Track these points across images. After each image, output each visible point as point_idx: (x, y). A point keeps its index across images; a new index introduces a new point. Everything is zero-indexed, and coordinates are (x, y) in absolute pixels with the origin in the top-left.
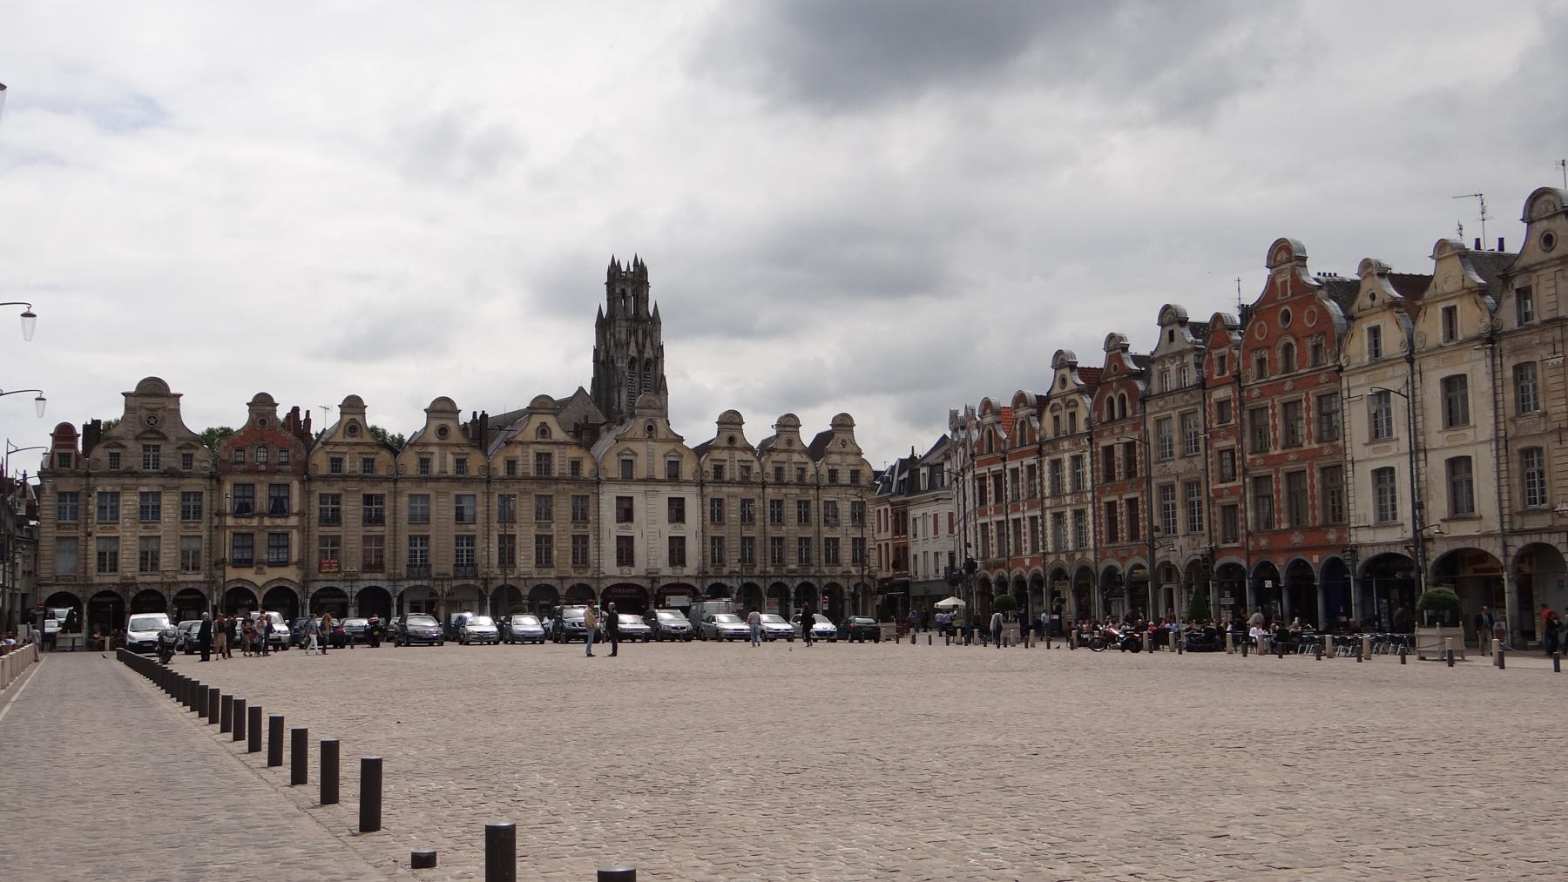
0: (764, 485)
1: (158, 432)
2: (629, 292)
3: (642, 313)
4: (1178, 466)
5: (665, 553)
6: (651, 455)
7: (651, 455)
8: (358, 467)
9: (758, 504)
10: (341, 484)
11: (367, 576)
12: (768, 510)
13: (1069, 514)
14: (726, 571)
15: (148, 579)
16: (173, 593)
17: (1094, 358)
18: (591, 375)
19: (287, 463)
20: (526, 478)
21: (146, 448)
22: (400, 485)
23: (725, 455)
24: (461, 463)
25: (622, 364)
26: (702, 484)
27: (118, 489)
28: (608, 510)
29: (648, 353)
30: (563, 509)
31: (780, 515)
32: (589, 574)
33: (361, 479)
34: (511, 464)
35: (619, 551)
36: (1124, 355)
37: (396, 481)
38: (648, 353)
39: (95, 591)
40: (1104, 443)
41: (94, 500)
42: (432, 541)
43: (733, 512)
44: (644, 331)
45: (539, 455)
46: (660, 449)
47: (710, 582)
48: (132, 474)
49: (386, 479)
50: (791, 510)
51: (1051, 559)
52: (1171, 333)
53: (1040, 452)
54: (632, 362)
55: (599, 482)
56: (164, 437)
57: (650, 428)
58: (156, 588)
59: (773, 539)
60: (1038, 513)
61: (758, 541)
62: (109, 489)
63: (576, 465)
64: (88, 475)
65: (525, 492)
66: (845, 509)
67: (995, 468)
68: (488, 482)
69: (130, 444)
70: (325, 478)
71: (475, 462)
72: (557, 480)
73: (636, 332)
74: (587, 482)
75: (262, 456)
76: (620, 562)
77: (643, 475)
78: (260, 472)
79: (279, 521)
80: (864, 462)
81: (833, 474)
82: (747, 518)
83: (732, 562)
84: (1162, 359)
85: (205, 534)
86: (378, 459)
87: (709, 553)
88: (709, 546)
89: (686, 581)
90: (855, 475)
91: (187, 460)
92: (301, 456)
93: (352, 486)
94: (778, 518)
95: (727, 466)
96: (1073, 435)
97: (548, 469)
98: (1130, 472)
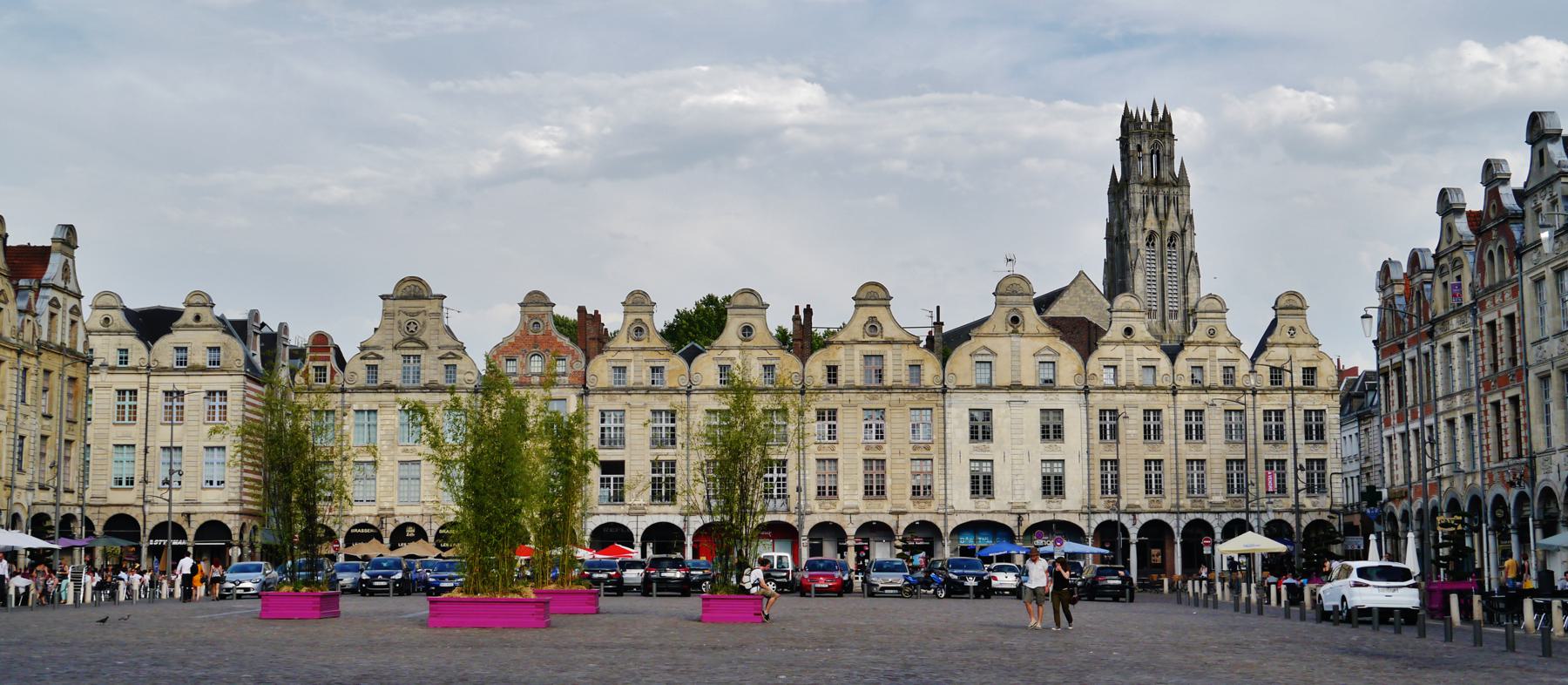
0: (1174, 391)
1: (418, 341)
2: (1146, 149)
3: (1165, 175)
4: (1553, 347)
5: (1037, 483)
6: (1016, 354)
7: (1016, 354)
8: (646, 379)
9: (1167, 415)
10: (626, 398)
11: (655, 509)
13: (1460, 422)
14: (1123, 507)
15: (407, 510)
16: (435, 527)
17: (1475, 200)
19: (564, 374)
20: (851, 387)
22: (693, 397)
23: (1120, 351)
24: (769, 368)
25: (1137, 240)
26: (1086, 391)
27: (375, 407)
28: (958, 427)
29: (1173, 225)
31: (1200, 429)
32: (934, 507)
33: (648, 391)
34: (832, 372)
35: (974, 479)
36: (1502, 190)
37: (688, 393)
38: (1173, 225)
40: (1487, 318)
41: (350, 419)
44: (1167, 198)
46: (1028, 346)
47: (1099, 519)
48: (389, 388)
49: (677, 391)
50: (1215, 424)
51: (1445, 485)
52: (1541, 153)
53: (1430, 334)
55: (944, 391)
56: (426, 347)
57: (1015, 320)
59: (1190, 461)
60: (1430, 421)
61: (1166, 466)
62: (366, 407)
63: (915, 367)
64: (343, 391)
65: (850, 405)
67: (1397, 359)
68: (802, 393)
69: (388, 354)
70: (606, 391)
71: (788, 364)
72: (889, 390)
73: (1155, 199)
74: (927, 389)
75: (536, 366)
76: (975, 491)
77: (1007, 382)
78: (530, 385)
80: (1321, 356)
82: (1152, 432)
83: (1133, 491)
84: (1534, 191)
86: (668, 366)
87: (1097, 482)
88: (1097, 472)
89: (1065, 517)
90: (1310, 374)
92: (579, 367)
93: (636, 399)
94: (1195, 432)
95: (1122, 366)
96: (1459, 311)
97: (880, 375)
98: (1513, 360)
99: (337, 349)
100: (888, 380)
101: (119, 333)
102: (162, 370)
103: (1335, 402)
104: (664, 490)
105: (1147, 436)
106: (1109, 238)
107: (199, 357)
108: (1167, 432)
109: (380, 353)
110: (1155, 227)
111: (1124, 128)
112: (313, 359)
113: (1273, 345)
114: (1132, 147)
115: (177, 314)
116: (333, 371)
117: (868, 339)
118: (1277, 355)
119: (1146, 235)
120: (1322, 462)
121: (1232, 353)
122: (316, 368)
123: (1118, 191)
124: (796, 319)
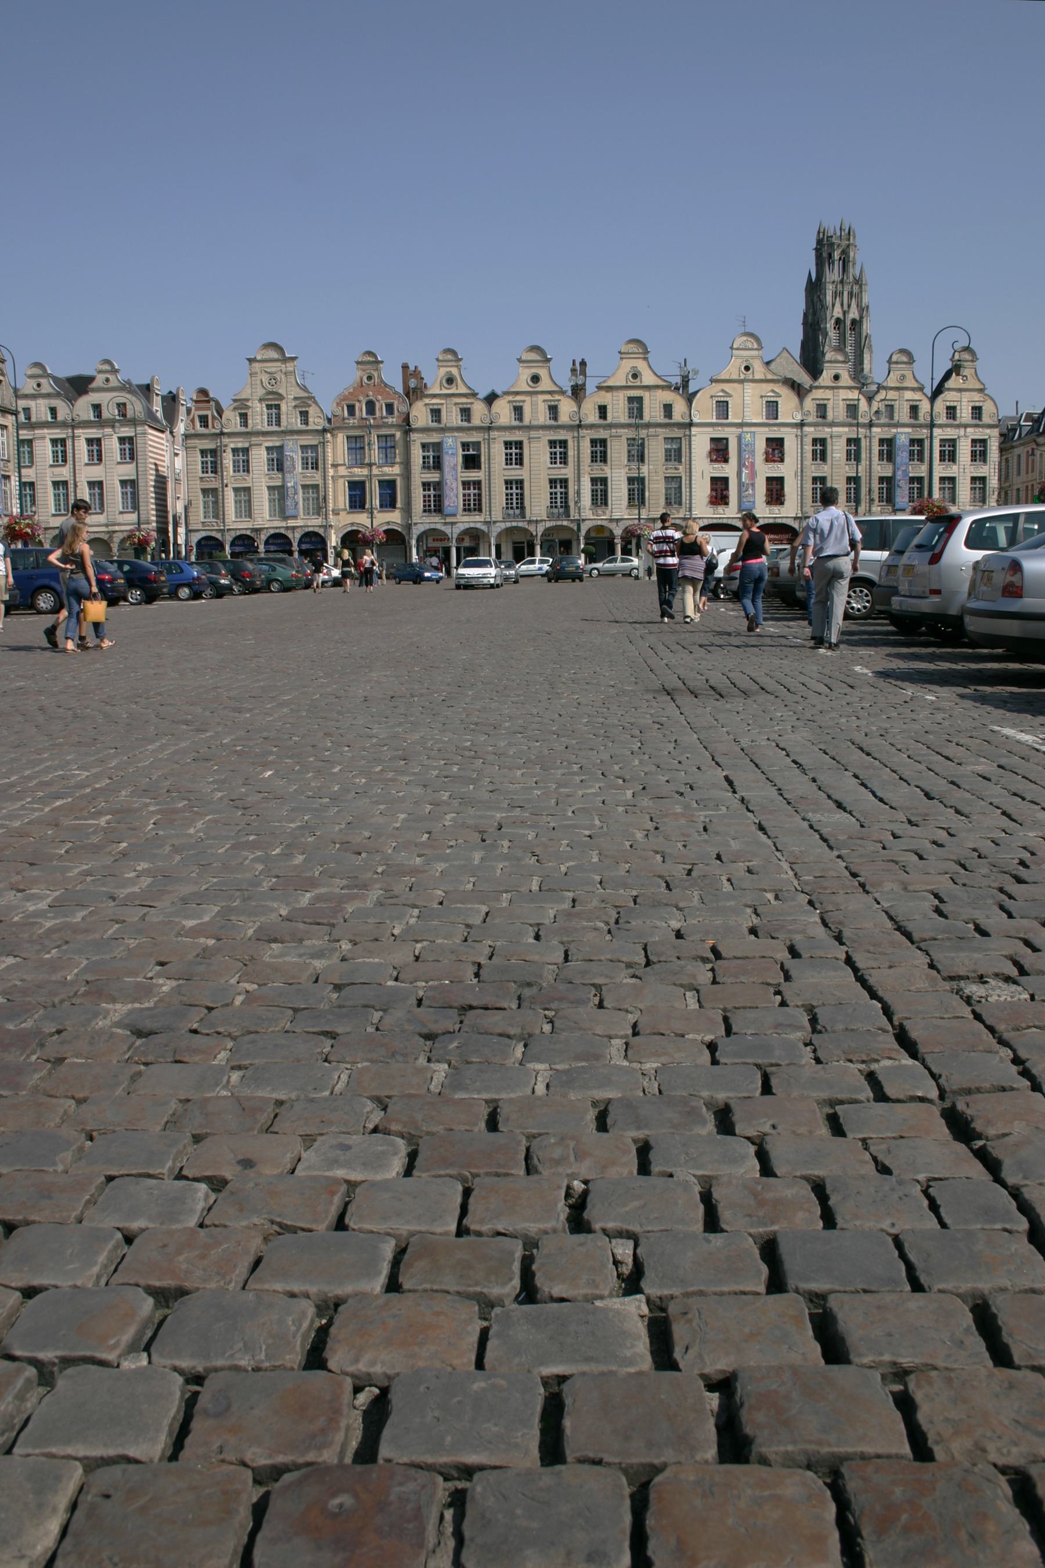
0: (871, 425)
11: (466, 519)
12: (876, 449)
18: (801, 337)
21: (269, 407)
23: (828, 394)
24: (554, 410)
27: (246, 445)
29: (854, 314)
30: (656, 449)
34: (603, 411)
37: (489, 429)
39: (233, 534)
42: (526, 485)
43: (838, 450)
44: (851, 294)
45: (631, 400)
54: (838, 321)
55: (691, 424)
56: (281, 397)
57: (747, 368)
58: (283, 531)
62: (240, 445)
63: (668, 409)
64: (222, 434)
66: (964, 450)
79: (387, 470)
81: (951, 411)
85: (320, 482)
89: (784, 521)
90: (977, 411)
91: (304, 415)
99: (217, 403)
100: (646, 418)
101: (48, 396)
102: (86, 424)
103: (995, 432)
104: (474, 505)
105: (848, 459)
106: (805, 323)
107: (110, 412)
108: (863, 455)
109: (249, 404)
110: (841, 316)
111: (819, 242)
112: (197, 409)
113: (949, 389)
114: (825, 255)
115: (91, 379)
116: (214, 417)
117: (630, 384)
118: (948, 398)
119: (833, 321)
120: (983, 480)
121: (917, 396)
122: (200, 417)
123: (814, 288)
124: (573, 370)
